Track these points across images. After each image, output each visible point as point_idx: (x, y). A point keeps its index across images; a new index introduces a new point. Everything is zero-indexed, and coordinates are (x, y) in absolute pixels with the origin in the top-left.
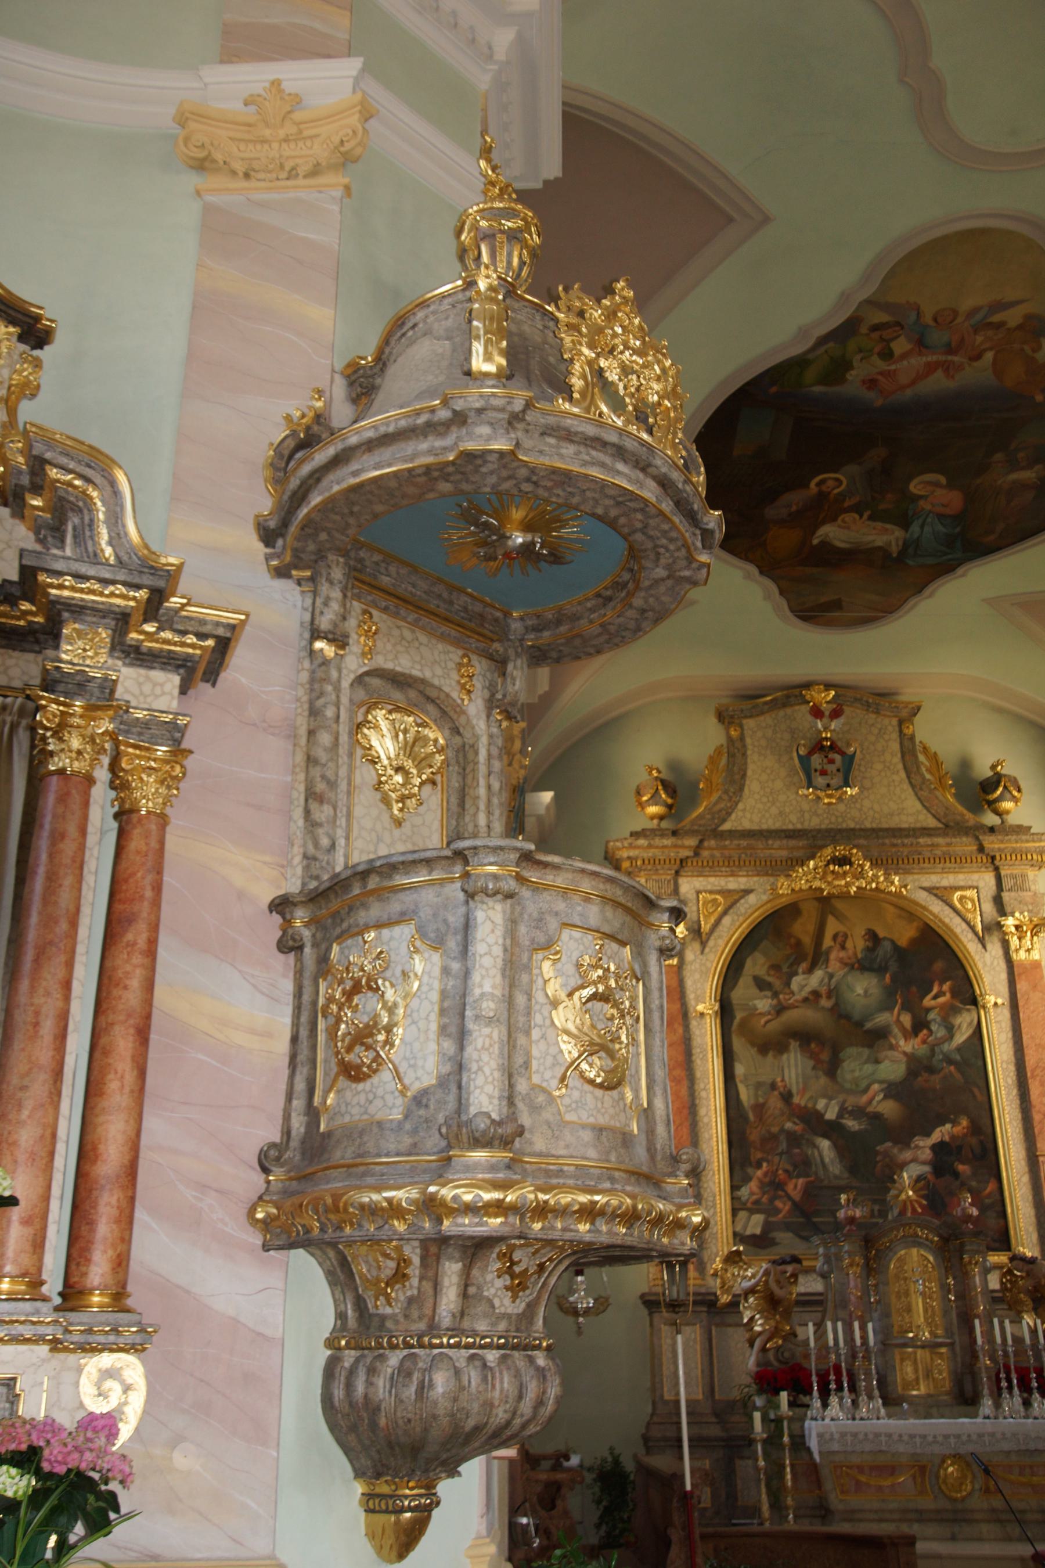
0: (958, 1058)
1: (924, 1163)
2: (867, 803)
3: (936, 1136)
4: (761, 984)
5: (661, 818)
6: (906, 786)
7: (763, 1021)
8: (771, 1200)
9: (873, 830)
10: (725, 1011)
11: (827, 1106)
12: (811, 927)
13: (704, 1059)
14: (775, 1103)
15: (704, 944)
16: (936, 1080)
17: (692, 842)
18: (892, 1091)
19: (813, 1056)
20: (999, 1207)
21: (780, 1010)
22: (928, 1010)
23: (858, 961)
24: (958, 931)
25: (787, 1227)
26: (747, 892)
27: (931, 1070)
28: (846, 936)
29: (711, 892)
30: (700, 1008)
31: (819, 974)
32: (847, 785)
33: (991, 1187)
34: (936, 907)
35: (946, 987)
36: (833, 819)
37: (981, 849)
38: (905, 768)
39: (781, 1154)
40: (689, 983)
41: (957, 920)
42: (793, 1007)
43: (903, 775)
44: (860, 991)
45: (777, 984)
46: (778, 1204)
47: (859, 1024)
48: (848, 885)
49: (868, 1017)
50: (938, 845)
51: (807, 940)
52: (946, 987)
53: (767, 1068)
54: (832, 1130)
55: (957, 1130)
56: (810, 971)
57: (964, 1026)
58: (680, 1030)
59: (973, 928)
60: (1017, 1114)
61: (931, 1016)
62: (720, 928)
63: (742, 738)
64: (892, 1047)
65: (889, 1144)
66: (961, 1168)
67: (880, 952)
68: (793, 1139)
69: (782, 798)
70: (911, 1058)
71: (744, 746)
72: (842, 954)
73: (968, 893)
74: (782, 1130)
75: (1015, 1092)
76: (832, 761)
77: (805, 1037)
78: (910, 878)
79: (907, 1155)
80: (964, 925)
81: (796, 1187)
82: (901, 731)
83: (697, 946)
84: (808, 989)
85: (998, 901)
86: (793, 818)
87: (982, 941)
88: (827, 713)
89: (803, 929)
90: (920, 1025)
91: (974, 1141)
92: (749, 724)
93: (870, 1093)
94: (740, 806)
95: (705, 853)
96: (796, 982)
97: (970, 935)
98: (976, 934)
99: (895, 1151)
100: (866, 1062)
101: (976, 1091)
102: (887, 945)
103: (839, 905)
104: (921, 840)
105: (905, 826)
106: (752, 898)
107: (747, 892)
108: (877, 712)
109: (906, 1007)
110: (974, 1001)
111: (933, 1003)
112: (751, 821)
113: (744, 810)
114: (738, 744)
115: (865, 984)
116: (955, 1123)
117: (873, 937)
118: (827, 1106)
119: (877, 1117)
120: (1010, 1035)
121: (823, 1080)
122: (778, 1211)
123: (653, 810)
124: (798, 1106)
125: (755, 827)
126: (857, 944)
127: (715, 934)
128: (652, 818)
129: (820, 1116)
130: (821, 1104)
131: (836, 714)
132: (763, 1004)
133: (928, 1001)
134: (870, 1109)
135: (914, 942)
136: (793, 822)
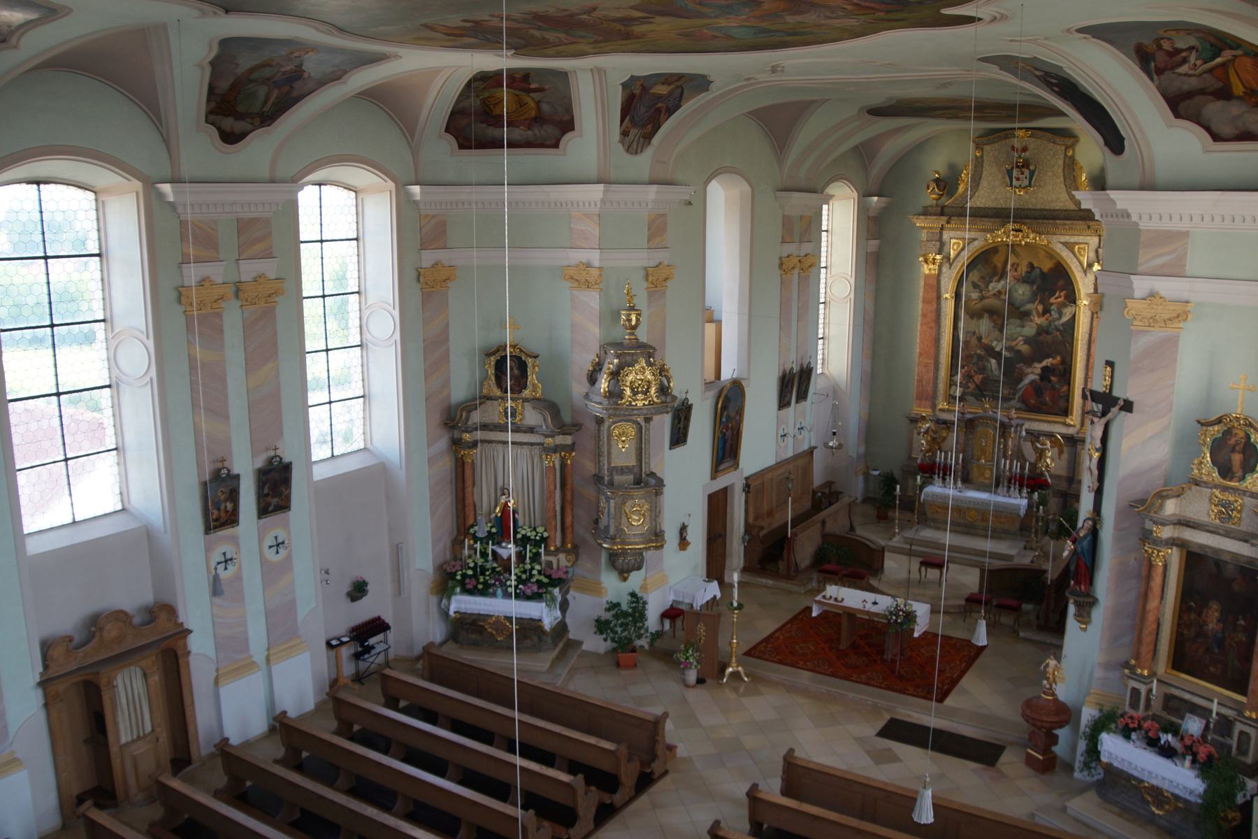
0: (1061, 328)
1: (1037, 374)
2: (1040, 195)
3: (1044, 363)
4: (975, 286)
5: (938, 199)
6: (1063, 186)
7: (973, 303)
8: (967, 382)
9: (1041, 210)
10: (958, 296)
11: (997, 345)
12: (1002, 259)
13: (945, 318)
14: (974, 341)
15: (951, 265)
16: (1049, 338)
17: (945, 218)
18: (1028, 341)
19: (994, 321)
20: (1068, 398)
21: (982, 298)
22: (1052, 304)
23: (1023, 278)
24: (1073, 267)
25: (972, 395)
26: (974, 240)
27: (1047, 333)
28: (1018, 265)
29: (957, 239)
30: (947, 296)
31: (1002, 282)
32: (1030, 185)
33: (1065, 388)
34: (1065, 254)
35: (1062, 294)
36: (1021, 203)
37: (1089, 227)
38: (1064, 175)
39: (973, 364)
40: (943, 283)
41: (1075, 260)
42: (988, 298)
43: (1062, 179)
44: (1021, 292)
45: (982, 286)
46: (970, 385)
47: (1017, 308)
48: (1020, 241)
49: (1023, 305)
50: (1066, 224)
51: (999, 266)
52: (1062, 294)
53: (973, 324)
54: (997, 355)
55: (1055, 362)
56: (998, 281)
57: (1068, 313)
58: (935, 306)
59: (1081, 264)
60: (1085, 357)
61: (1053, 307)
62: (960, 257)
63: (982, 157)
64: (1031, 321)
65: (1022, 365)
66: (1053, 378)
67: (1033, 274)
68: (980, 358)
69: (997, 190)
70: (1040, 327)
71: (983, 161)
72: (1015, 274)
73: (1082, 246)
74: (976, 354)
75: (1086, 347)
76: (1023, 173)
77: (993, 313)
78: (1055, 236)
79: (1029, 370)
80: (1078, 263)
81: (978, 378)
82: (1066, 155)
83: (948, 265)
84: (996, 290)
85: (1097, 252)
86: (1002, 202)
87: (1085, 272)
88: (1020, 149)
89: (997, 260)
90: (1046, 311)
91: (1061, 367)
92: (987, 148)
93: (1017, 341)
94: (977, 194)
95: (953, 222)
96: (992, 285)
97: (1080, 269)
98: (1083, 267)
99: (1024, 368)
100: (1018, 326)
101: (1067, 345)
102: (1037, 271)
103: (1018, 249)
104: (1058, 222)
105: (1058, 208)
106: (976, 243)
107: (974, 240)
108: (1054, 143)
109: (1041, 302)
110: (1075, 303)
111: (1055, 301)
112: (981, 202)
113: (978, 196)
114: (980, 160)
115: (1023, 289)
116: (1054, 358)
117: (1031, 266)
118: (997, 345)
119: (1019, 351)
120: (1089, 320)
121: (997, 333)
122: (969, 387)
123: (934, 196)
124: (985, 345)
125: (982, 206)
126: (1023, 269)
127: (957, 259)
128: (934, 199)
129: (993, 349)
130: (994, 344)
131: (1024, 149)
132: (975, 295)
133: (1052, 300)
134: (1016, 348)
135: (1051, 270)
136: (1001, 204)
